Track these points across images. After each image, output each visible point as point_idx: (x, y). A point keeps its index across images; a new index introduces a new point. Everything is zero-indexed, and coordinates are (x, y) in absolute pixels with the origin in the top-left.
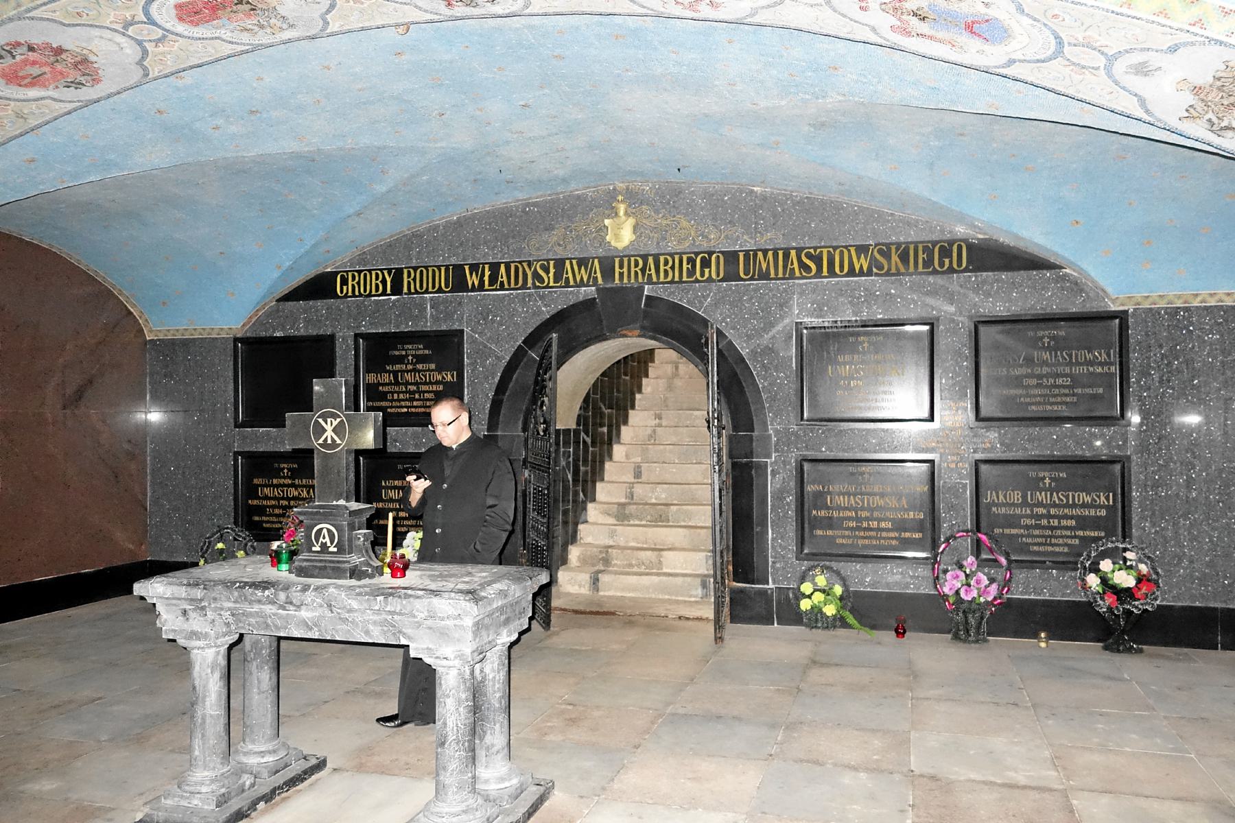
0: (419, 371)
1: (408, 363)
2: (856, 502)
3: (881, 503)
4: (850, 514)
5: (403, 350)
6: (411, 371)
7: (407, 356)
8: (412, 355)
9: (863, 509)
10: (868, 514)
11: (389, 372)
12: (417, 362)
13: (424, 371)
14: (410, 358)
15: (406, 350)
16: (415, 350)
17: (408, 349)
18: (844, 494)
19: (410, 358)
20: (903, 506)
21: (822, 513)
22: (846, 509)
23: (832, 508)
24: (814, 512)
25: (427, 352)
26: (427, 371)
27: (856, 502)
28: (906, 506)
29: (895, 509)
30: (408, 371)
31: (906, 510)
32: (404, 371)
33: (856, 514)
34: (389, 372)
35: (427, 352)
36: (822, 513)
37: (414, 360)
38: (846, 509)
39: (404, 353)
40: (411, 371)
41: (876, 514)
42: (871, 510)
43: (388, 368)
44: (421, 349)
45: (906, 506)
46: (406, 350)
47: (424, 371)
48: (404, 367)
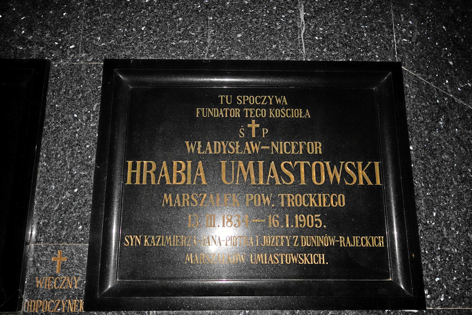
0: (278, 158)
1: (248, 138)
5: (234, 105)
6: (255, 157)
7: (245, 120)
8: (259, 120)
11: (195, 158)
12: (273, 136)
13: (294, 158)
14: (254, 125)
15: (242, 107)
16: (267, 107)
17: (248, 105)
19: (254, 125)
25: (298, 113)
26: (301, 158)
30: (246, 158)
32: (237, 158)
34: (195, 158)
35: (298, 113)
37: (265, 131)
39: (236, 113)
40: (255, 157)
43: (190, 148)
44: (279, 106)
46: (242, 107)
47: (294, 158)
48: (235, 148)
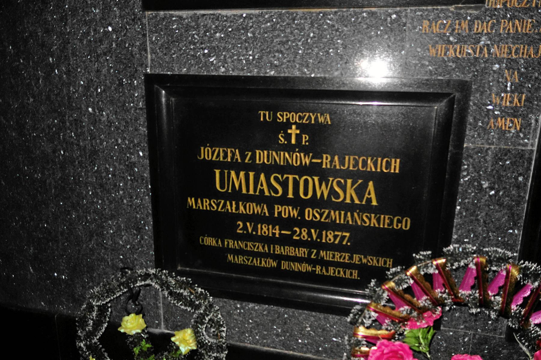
2: (270, 185)
3: (323, 191)
4: (258, 210)
9: (283, 200)
10: (295, 213)
18: (247, 168)
20: (369, 200)
21: (206, 204)
22: (248, 198)
23: (226, 196)
24: (191, 201)
27: (270, 185)
28: (374, 203)
29: (351, 208)
31: (376, 211)
33: (271, 210)
36: (206, 204)
38: (248, 198)
41: (310, 214)
42: (297, 202)
45: (374, 203)
